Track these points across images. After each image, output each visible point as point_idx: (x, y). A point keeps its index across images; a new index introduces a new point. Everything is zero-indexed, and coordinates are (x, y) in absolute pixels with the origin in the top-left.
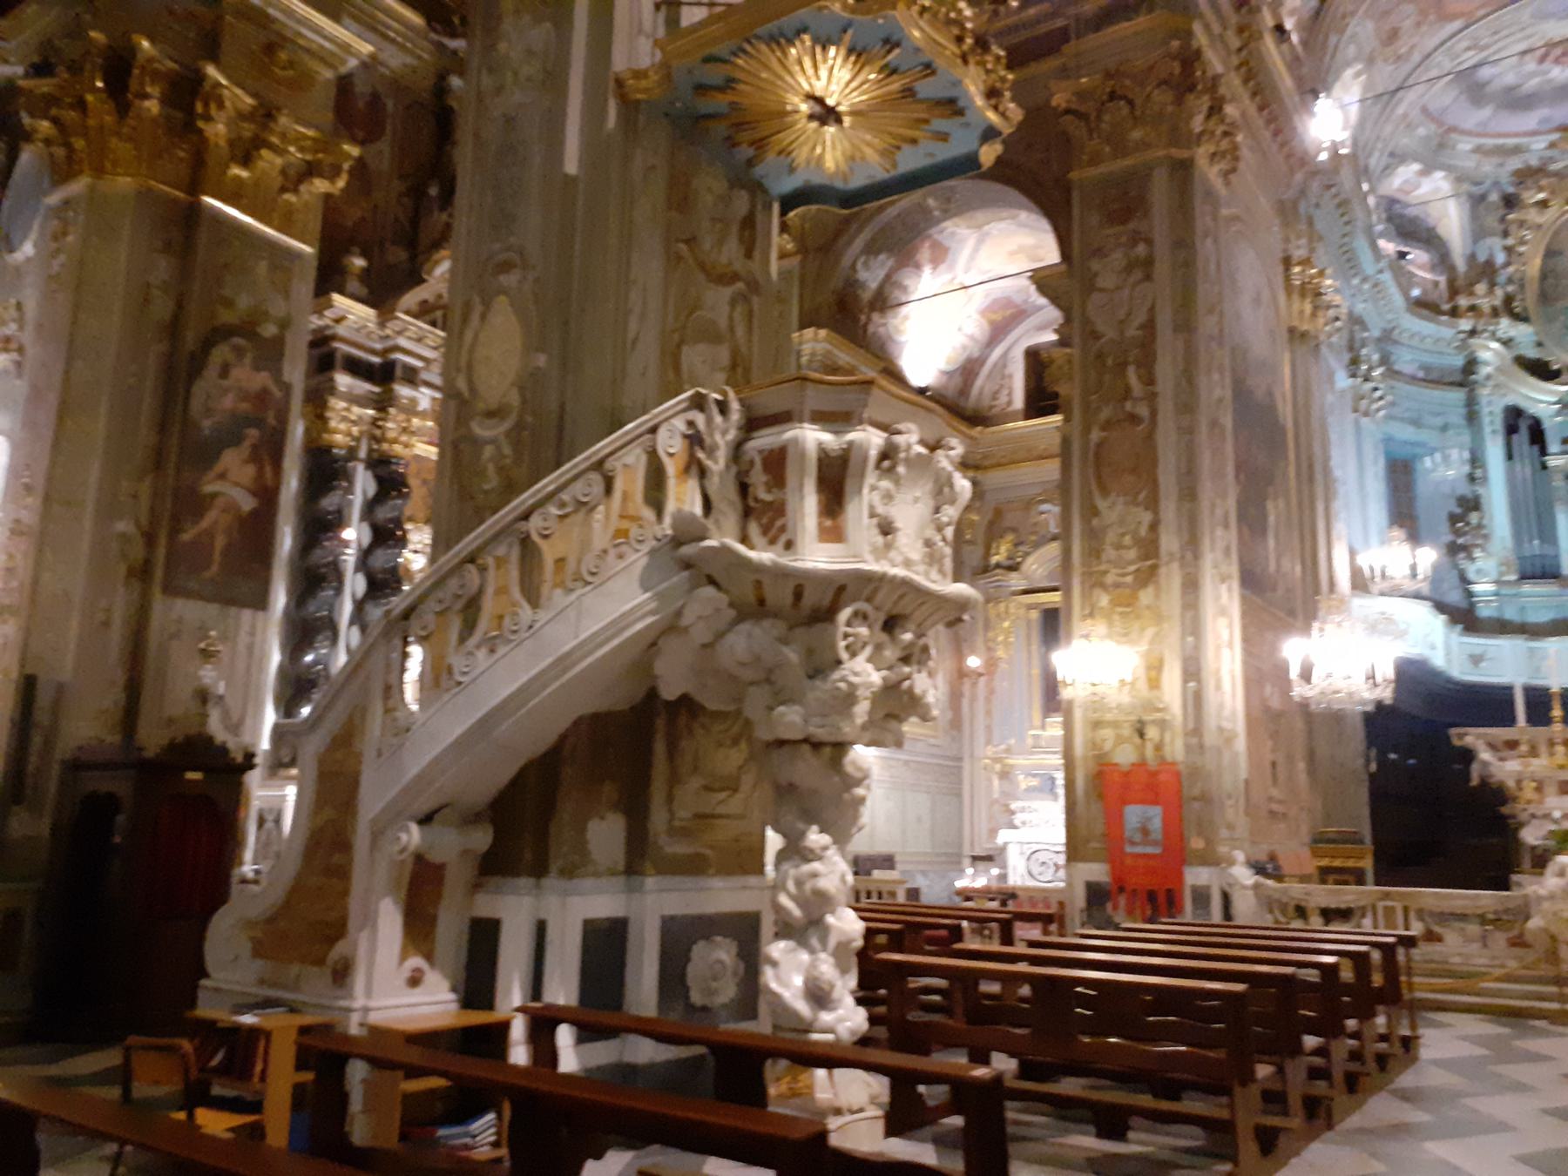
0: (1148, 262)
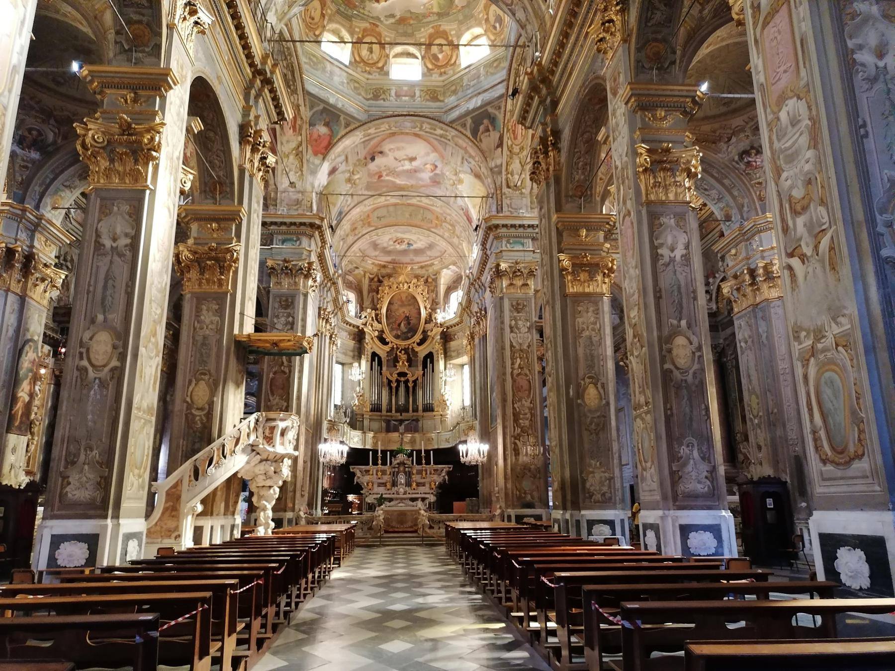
0: (292, 324)
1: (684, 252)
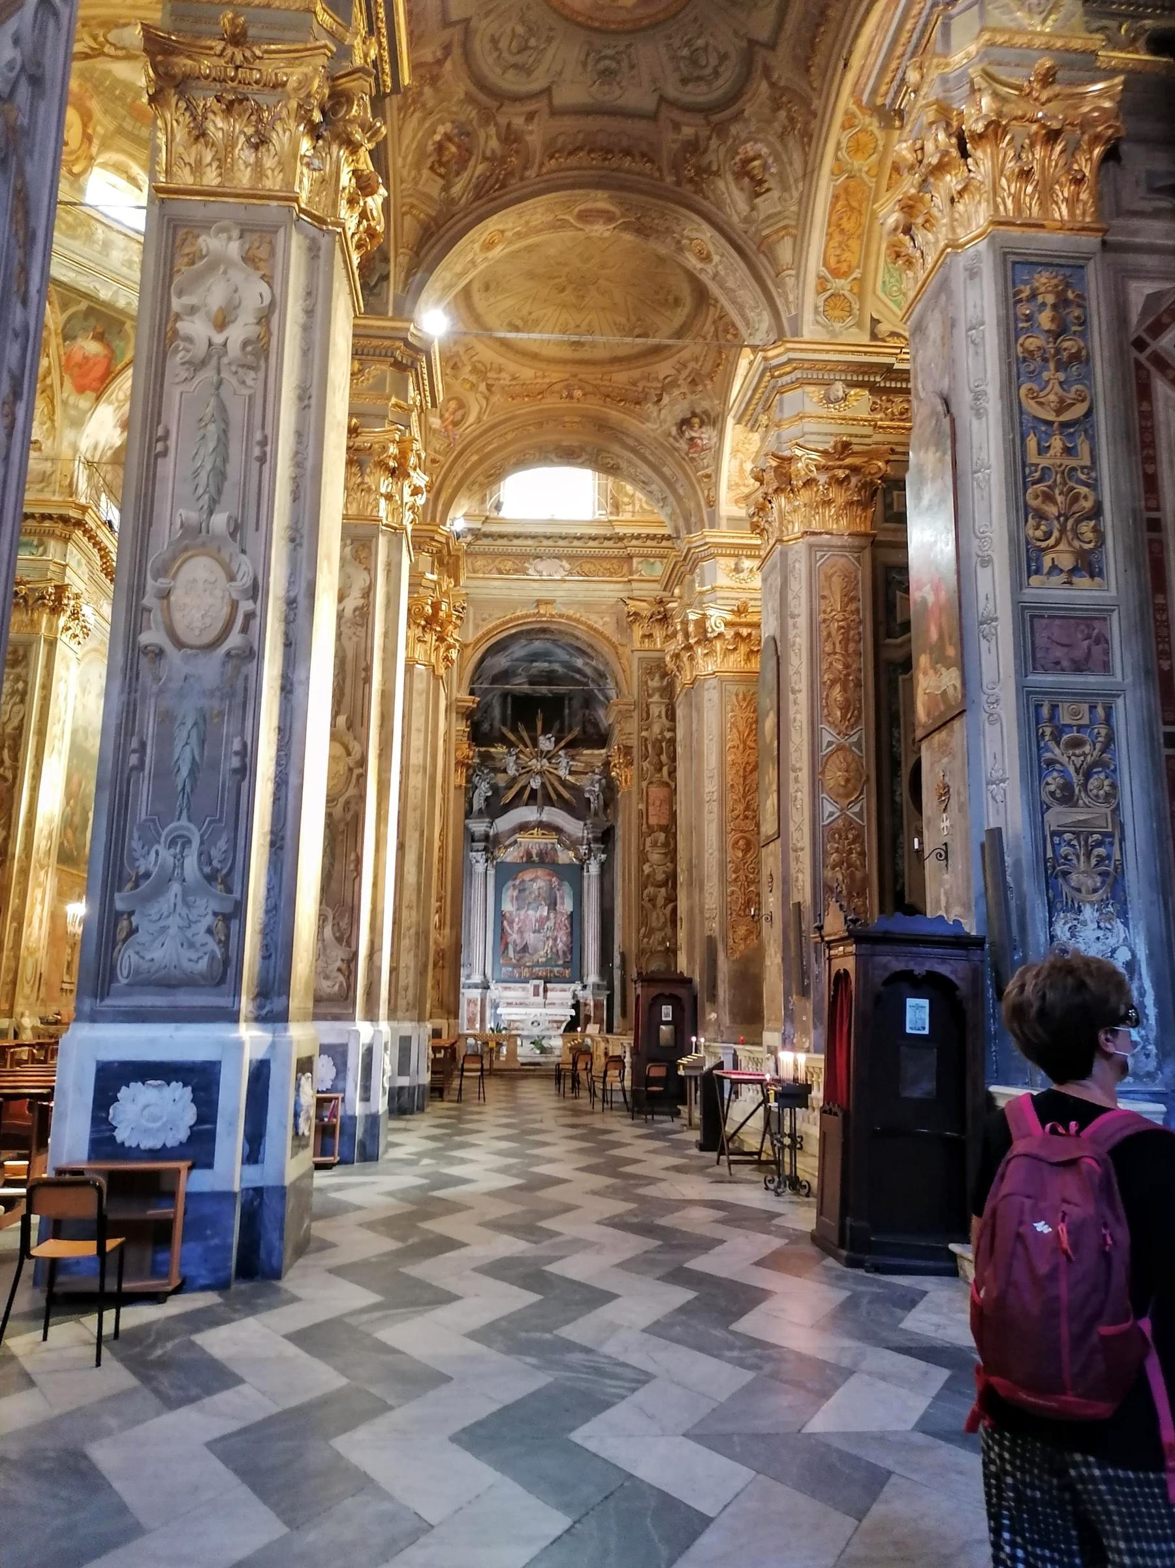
1: (360, 602)
